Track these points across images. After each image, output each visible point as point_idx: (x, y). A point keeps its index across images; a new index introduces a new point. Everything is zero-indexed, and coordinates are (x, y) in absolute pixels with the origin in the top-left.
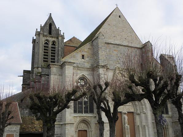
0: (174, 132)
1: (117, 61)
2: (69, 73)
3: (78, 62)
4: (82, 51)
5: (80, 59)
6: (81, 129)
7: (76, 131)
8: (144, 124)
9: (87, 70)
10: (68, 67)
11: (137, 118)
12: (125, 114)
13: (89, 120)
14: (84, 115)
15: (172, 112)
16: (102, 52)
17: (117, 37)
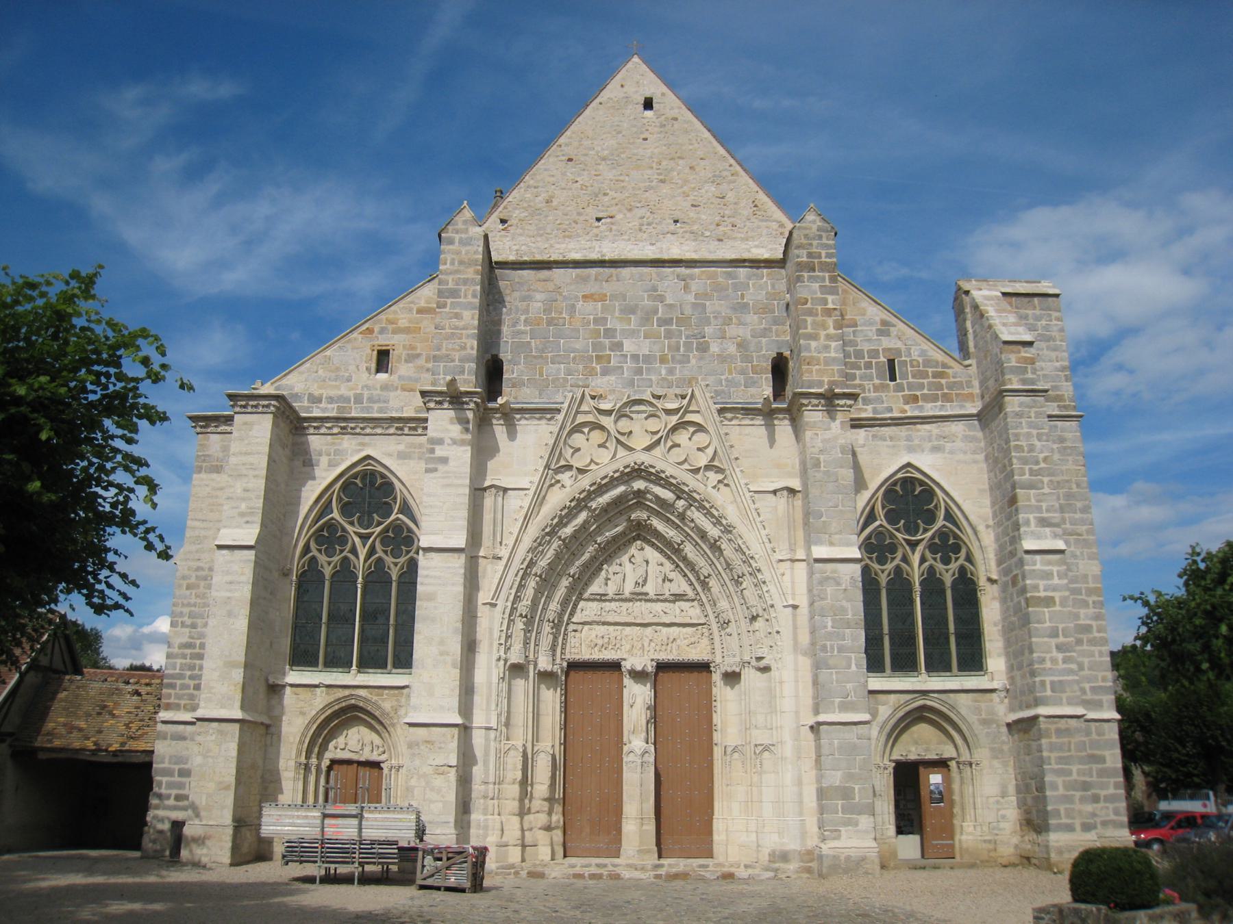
2: (246, 454)
3: (351, 394)
4: (376, 329)
10: (245, 424)
11: (727, 702)
13: (387, 705)
14: (353, 677)
16: (458, 316)
17: (619, 217)
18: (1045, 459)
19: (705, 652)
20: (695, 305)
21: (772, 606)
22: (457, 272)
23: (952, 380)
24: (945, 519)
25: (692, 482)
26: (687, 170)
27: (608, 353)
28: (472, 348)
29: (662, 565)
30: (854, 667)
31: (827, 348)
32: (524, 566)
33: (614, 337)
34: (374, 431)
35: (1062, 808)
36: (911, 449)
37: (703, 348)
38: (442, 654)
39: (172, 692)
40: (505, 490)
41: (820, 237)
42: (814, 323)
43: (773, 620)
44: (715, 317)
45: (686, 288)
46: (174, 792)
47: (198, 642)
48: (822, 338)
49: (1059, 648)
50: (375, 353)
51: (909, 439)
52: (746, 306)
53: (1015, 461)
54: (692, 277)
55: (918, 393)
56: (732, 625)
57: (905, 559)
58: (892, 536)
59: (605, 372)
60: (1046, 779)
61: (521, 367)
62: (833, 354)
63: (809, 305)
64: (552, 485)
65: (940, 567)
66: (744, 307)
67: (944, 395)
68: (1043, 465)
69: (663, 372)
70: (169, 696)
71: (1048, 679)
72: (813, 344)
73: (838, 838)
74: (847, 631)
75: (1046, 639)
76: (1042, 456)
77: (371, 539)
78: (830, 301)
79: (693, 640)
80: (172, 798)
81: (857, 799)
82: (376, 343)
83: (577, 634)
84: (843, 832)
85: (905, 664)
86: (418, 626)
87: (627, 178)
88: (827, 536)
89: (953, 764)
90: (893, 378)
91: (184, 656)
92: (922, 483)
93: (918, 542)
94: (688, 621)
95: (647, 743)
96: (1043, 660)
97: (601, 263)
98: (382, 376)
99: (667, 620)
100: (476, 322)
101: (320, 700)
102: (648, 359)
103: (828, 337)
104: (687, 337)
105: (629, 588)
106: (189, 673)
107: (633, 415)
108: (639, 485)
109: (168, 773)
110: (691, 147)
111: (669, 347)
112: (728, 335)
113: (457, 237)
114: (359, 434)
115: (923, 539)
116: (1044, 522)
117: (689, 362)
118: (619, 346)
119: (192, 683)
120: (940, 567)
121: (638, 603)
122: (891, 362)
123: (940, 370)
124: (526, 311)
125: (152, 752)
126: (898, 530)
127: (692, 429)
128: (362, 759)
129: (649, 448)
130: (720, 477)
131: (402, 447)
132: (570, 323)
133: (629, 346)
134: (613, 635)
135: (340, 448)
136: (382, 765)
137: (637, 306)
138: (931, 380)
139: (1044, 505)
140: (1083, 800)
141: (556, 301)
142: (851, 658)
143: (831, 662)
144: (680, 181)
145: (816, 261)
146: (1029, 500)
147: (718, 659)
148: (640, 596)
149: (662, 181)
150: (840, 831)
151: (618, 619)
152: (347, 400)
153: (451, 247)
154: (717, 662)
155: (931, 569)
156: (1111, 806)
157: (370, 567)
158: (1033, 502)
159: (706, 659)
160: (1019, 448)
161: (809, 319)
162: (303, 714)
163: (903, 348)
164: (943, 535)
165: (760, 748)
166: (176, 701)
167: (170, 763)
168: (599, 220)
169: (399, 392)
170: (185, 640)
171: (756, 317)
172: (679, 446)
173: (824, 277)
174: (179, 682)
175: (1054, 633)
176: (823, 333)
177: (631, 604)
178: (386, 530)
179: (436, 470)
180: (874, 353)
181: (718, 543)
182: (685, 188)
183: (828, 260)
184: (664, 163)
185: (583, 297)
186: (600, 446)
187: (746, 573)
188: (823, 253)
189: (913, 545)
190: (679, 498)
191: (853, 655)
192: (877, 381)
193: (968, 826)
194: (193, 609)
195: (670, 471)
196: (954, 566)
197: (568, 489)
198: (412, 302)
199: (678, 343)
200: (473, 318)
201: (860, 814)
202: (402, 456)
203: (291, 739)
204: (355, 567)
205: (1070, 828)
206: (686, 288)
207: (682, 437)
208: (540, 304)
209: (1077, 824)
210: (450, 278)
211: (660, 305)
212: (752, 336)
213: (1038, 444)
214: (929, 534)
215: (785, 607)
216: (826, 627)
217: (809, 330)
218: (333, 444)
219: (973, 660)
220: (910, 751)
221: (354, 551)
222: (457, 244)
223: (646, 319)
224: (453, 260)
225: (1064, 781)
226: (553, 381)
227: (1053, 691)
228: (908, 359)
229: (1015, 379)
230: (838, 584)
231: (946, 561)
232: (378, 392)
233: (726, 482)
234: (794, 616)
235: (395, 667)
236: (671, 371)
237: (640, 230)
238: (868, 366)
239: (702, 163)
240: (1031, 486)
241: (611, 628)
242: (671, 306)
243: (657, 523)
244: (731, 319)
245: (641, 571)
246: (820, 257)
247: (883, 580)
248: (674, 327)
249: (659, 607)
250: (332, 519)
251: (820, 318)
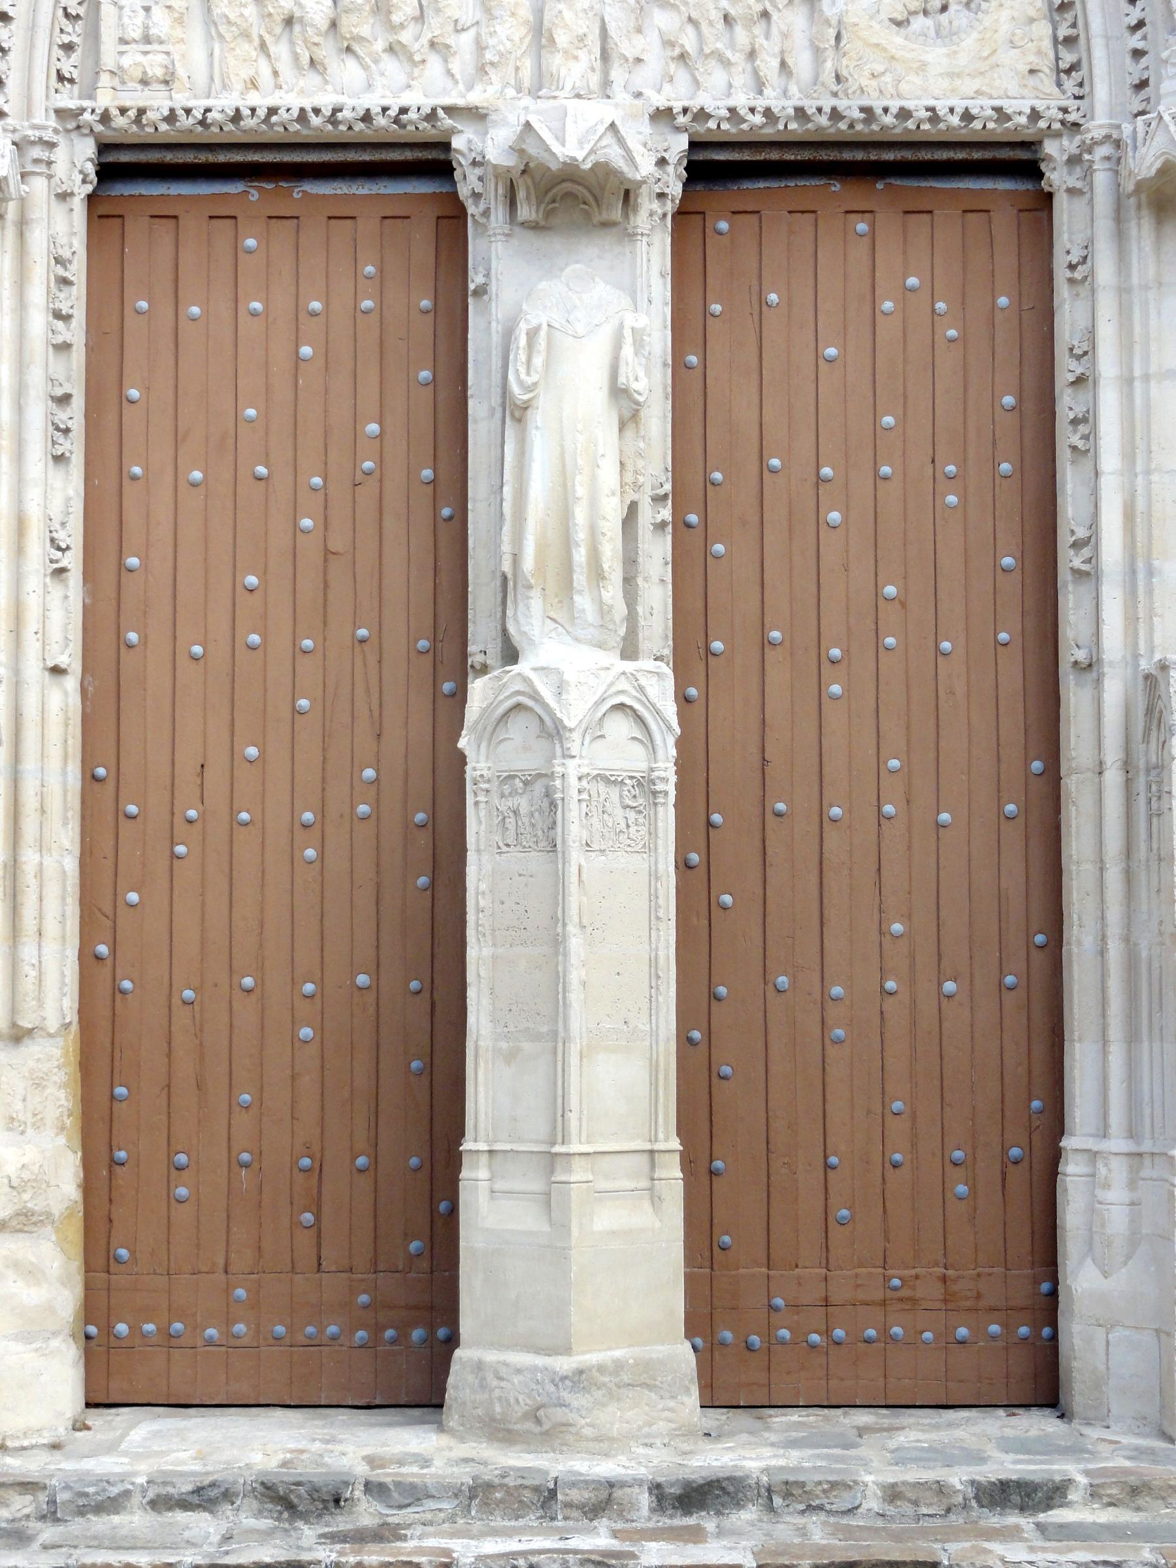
19: (1014, 61)
95: (629, 651)
154: (1097, 126)
159: (1019, 106)
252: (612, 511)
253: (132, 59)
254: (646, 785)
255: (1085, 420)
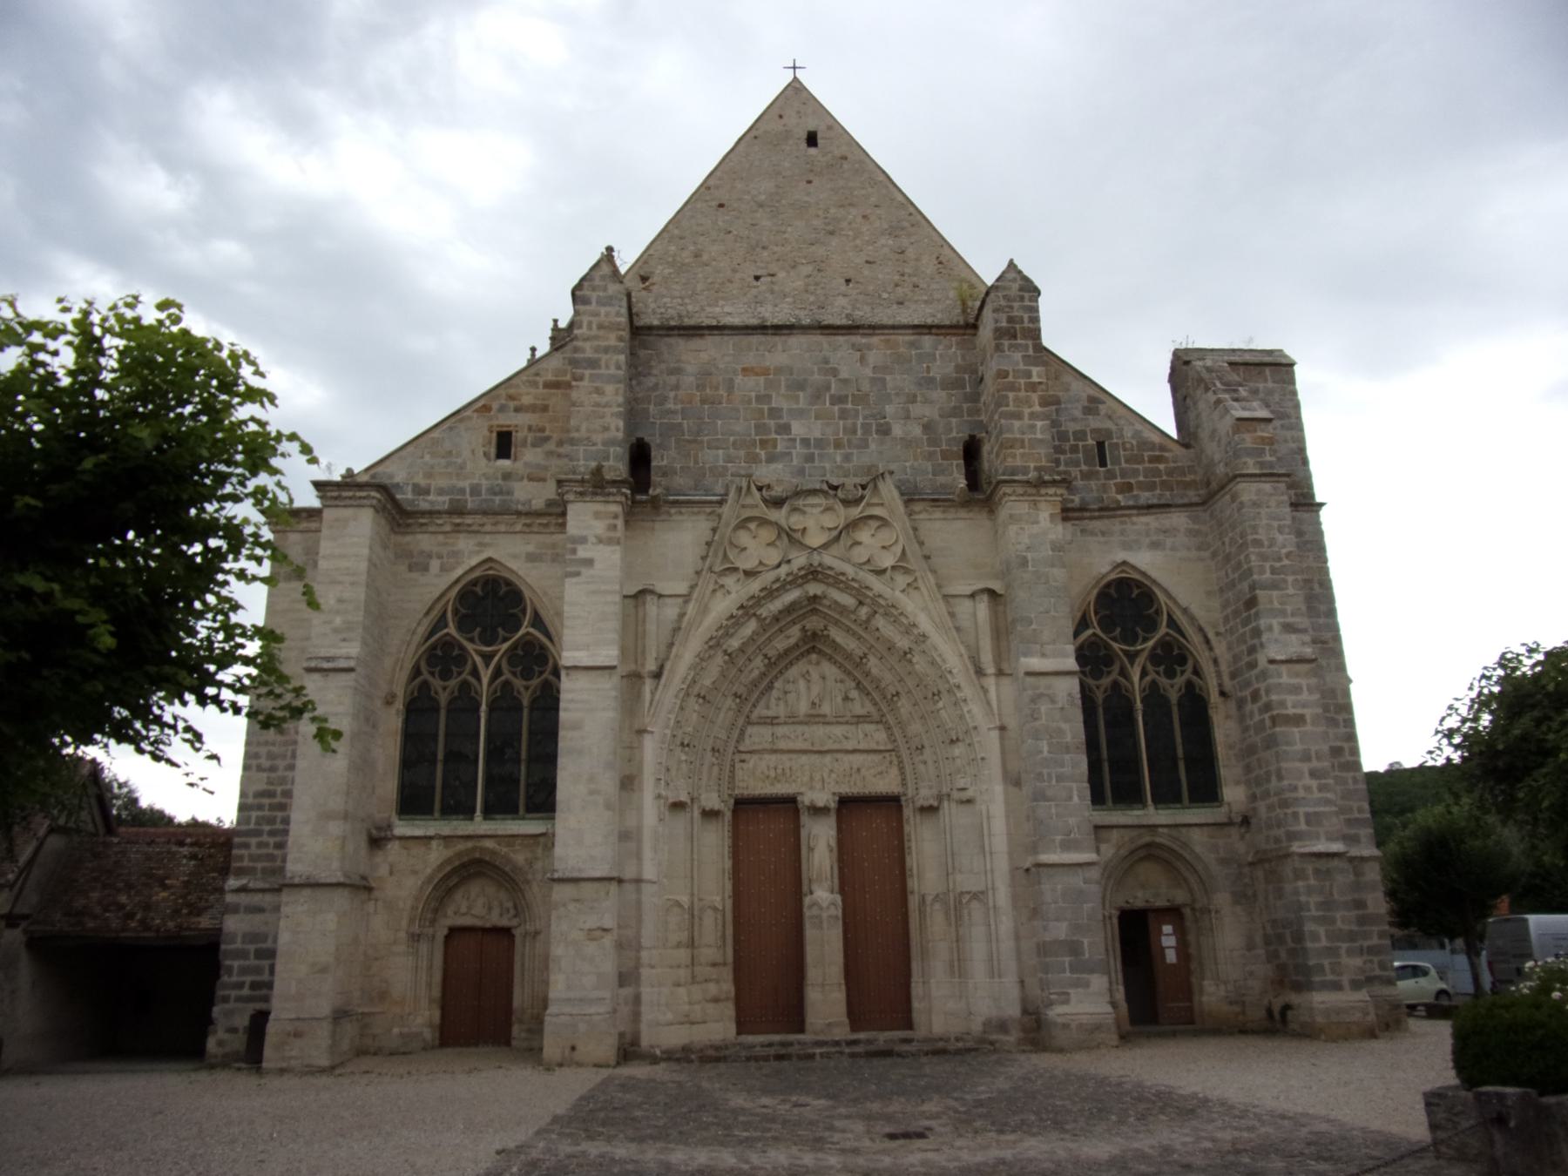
0: (1267, 941)
1: (763, 443)
4: (495, 406)
5: (484, 462)
6: (467, 921)
7: (415, 938)
8: (966, 882)
9: (528, 525)
10: (337, 520)
12: (817, 811)
13: (520, 858)
14: (480, 825)
15: (1248, 783)
16: (599, 391)
17: (781, 275)
18: (1288, 555)
20: (873, 381)
21: (975, 728)
22: (596, 338)
23: (1172, 465)
24: (1168, 626)
25: (877, 585)
26: (859, 219)
27: (774, 436)
28: (618, 430)
29: (842, 681)
30: (1076, 799)
31: (1033, 427)
32: (685, 686)
33: (781, 417)
34: (494, 529)
35: (1326, 963)
36: (1127, 546)
37: (885, 431)
38: (591, 793)
39: (244, 852)
40: (660, 596)
41: (1022, 299)
42: (1016, 399)
43: (976, 745)
44: (897, 394)
45: (862, 359)
46: (248, 979)
47: (279, 789)
48: (1026, 416)
49: (1314, 774)
50: (494, 435)
51: (1123, 533)
52: (931, 381)
53: (1253, 558)
54: (869, 347)
55: (1132, 481)
56: (927, 752)
57: (1123, 673)
58: (1107, 647)
59: (771, 459)
60: (1306, 928)
61: (673, 453)
62: (1039, 436)
63: (1010, 378)
64: (714, 591)
65: (1163, 681)
66: (930, 382)
67: (1163, 483)
68: (1286, 562)
69: (838, 459)
70: (241, 858)
71: (1301, 810)
72: (1017, 424)
73: (1066, 1002)
74: (1067, 757)
75: (1298, 764)
76: (1284, 551)
77: (496, 659)
78: (1034, 373)
79: (880, 769)
80: (247, 986)
81: (1087, 956)
82: (495, 422)
83: (745, 765)
84: (1072, 996)
85: (1127, 795)
86: (562, 761)
87: (789, 229)
88: (1038, 647)
89: (1187, 912)
90: (1103, 463)
91: (260, 807)
92: (1139, 584)
93: (1137, 653)
94: (874, 746)
95: (832, 892)
96: (1295, 789)
97: (762, 329)
98: (505, 463)
99: (849, 746)
100: (620, 399)
101: (436, 855)
102: (820, 443)
103: (1033, 416)
104: (865, 418)
105: (803, 708)
106: (267, 828)
107: (808, 509)
108: (814, 589)
109: (242, 954)
110: (863, 192)
111: (844, 428)
112: (912, 415)
113: (594, 296)
114: (478, 532)
115: (1142, 650)
116: (1289, 628)
117: (867, 446)
118: (785, 429)
119: (272, 840)
120: (1163, 681)
121: (815, 728)
122: (1100, 445)
123: (1157, 453)
124: (677, 387)
125: (220, 930)
126: (1112, 639)
127: (874, 524)
128: (488, 925)
129: (825, 546)
130: (910, 579)
131: (531, 548)
132: (729, 401)
133: (798, 428)
134: (788, 765)
135: (455, 549)
136: (514, 932)
137: (805, 380)
138: (1147, 465)
139: (1289, 608)
140: (1350, 952)
141: (710, 374)
142: (1071, 790)
143: (1049, 793)
144: (850, 233)
145: (1018, 326)
146: (1271, 602)
147: (910, 793)
148: (814, 718)
149: (832, 233)
150: (1068, 994)
151: (792, 746)
152: (462, 491)
153: (587, 307)
155: (1154, 683)
156: (1376, 959)
157: (495, 692)
158: (1276, 605)
160: (1258, 543)
161: (1011, 395)
162: (415, 872)
163: (1114, 428)
164: (1165, 645)
165: (968, 897)
166: (251, 864)
167: (243, 942)
168: (757, 278)
169: (525, 481)
170: (262, 787)
171: (944, 394)
172: (859, 543)
173: (1027, 346)
174: (253, 841)
175: (1306, 757)
176: (1027, 411)
177: (805, 728)
178: (514, 647)
179: (578, 574)
180: (1080, 435)
181: (909, 656)
182: (858, 242)
183: (1031, 325)
184: (833, 211)
185: (744, 370)
186: (769, 545)
187: (942, 690)
188: (1026, 317)
189: (1132, 657)
190: (861, 603)
191: (1074, 785)
192: (1084, 467)
193: (1209, 986)
194: (271, 748)
195: (850, 571)
196: (1180, 680)
197: (733, 595)
198: (537, 374)
199: (855, 425)
200: (617, 394)
201: (1092, 971)
202: (532, 558)
203: (401, 904)
204: (476, 693)
205: (1337, 986)
206: (862, 359)
207: (864, 535)
208: (692, 379)
209: (1345, 980)
210: (587, 346)
211: (833, 380)
212: (941, 416)
213: (1280, 538)
214: (1150, 643)
215: (989, 729)
216: (1041, 752)
217: (1011, 408)
218: (446, 544)
219: (1206, 790)
220: (1136, 897)
221: (475, 673)
222: (594, 304)
223: (817, 397)
224: (590, 323)
225: (1326, 931)
226: (711, 469)
227: (1308, 823)
228: (1120, 441)
229: (1250, 461)
230: (1053, 701)
231: (1171, 674)
232: (500, 482)
233: (915, 585)
234: (1002, 738)
235: (528, 810)
236: (847, 458)
237: (807, 291)
238: (1074, 449)
239: (878, 211)
240: (1274, 586)
241: (785, 757)
242: (845, 381)
243: (837, 635)
244: (915, 396)
245: (816, 690)
246: (1022, 322)
247: (1100, 697)
248: (850, 406)
249: (838, 731)
250: (447, 634)
251: (1022, 394)
252: (828, 868)
253: (741, 784)
254: (837, 917)
255: (910, 848)
